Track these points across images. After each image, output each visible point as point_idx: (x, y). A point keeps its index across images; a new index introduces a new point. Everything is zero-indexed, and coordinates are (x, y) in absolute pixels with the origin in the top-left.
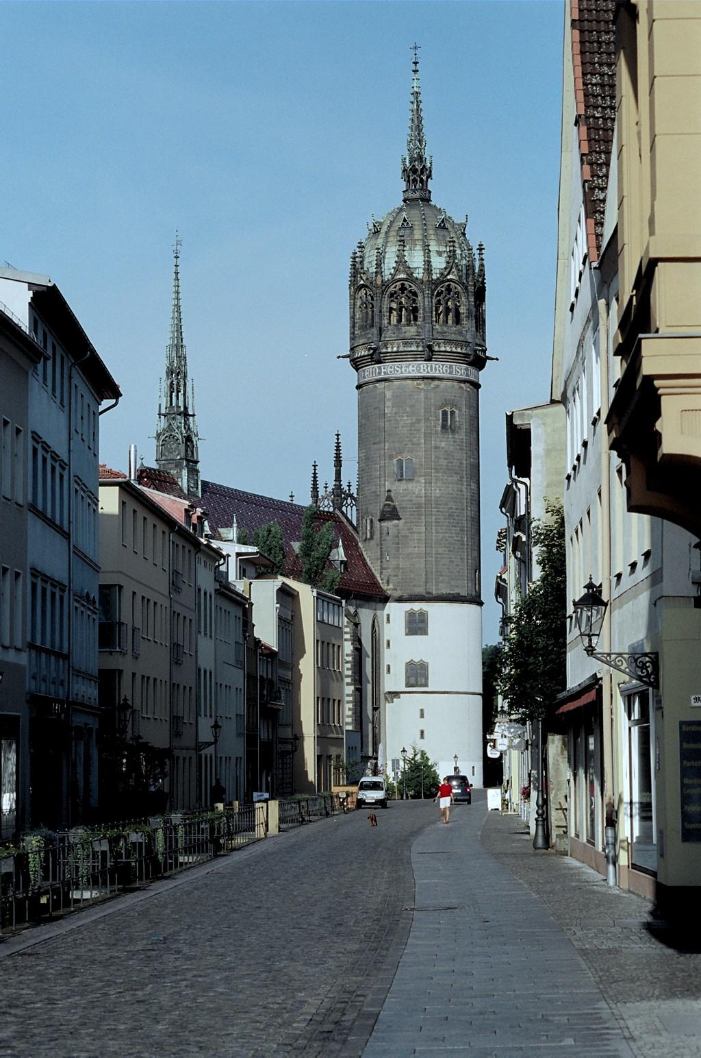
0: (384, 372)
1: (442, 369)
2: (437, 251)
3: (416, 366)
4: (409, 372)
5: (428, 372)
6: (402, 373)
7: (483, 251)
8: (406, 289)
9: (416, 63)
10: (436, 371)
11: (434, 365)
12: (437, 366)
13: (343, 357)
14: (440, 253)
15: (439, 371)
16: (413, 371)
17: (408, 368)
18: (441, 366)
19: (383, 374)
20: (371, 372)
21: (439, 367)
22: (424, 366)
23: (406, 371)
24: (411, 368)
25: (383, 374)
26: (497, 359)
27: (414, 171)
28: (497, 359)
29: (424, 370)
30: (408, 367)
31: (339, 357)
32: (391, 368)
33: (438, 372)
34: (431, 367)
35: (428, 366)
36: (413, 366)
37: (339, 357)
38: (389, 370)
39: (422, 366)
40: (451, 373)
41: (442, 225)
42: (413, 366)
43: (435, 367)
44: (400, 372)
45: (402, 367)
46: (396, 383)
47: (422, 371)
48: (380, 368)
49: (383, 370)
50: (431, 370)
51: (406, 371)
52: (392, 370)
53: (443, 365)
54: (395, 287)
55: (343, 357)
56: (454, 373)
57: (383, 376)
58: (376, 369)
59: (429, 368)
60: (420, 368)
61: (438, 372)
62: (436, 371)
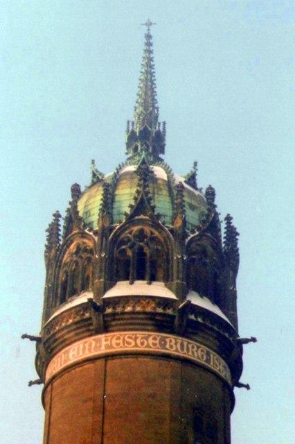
0: (107, 347)
1: (197, 351)
2: (188, 203)
3: (158, 339)
5: (177, 350)
6: (136, 345)
8: (146, 237)
9: (148, 37)
10: (188, 350)
11: (185, 344)
12: (190, 346)
13: (32, 338)
14: (192, 207)
15: (193, 353)
17: (147, 340)
18: (195, 349)
19: (103, 347)
20: (76, 352)
21: (193, 347)
22: (171, 341)
23: (142, 344)
24: (151, 341)
25: (103, 347)
27: (145, 134)
29: (171, 347)
30: (147, 339)
31: (25, 336)
32: (118, 338)
33: (190, 353)
34: (182, 345)
35: (176, 344)
36: (155, 339)
37: (25, 336)
38: (114, 341)
39: (168, 340)
40: (208, 361)
41: (192, 182)
43: (187, 346)
44: (133, 344)
45: (136, 339)
46: (125, 360)
47: (168, 346)
48: (99, 341)
49: (104, 343)
50: (182, 349)
52: (121, 341)
53: (198, 347)
54: (130, 233)
55: (32, 338)
56: (212, 364)
57: (103, 351)
58: (90, 345)
59: (179, 346)
60: (166, 343)
61: (190, 353)
62: (188, 350)
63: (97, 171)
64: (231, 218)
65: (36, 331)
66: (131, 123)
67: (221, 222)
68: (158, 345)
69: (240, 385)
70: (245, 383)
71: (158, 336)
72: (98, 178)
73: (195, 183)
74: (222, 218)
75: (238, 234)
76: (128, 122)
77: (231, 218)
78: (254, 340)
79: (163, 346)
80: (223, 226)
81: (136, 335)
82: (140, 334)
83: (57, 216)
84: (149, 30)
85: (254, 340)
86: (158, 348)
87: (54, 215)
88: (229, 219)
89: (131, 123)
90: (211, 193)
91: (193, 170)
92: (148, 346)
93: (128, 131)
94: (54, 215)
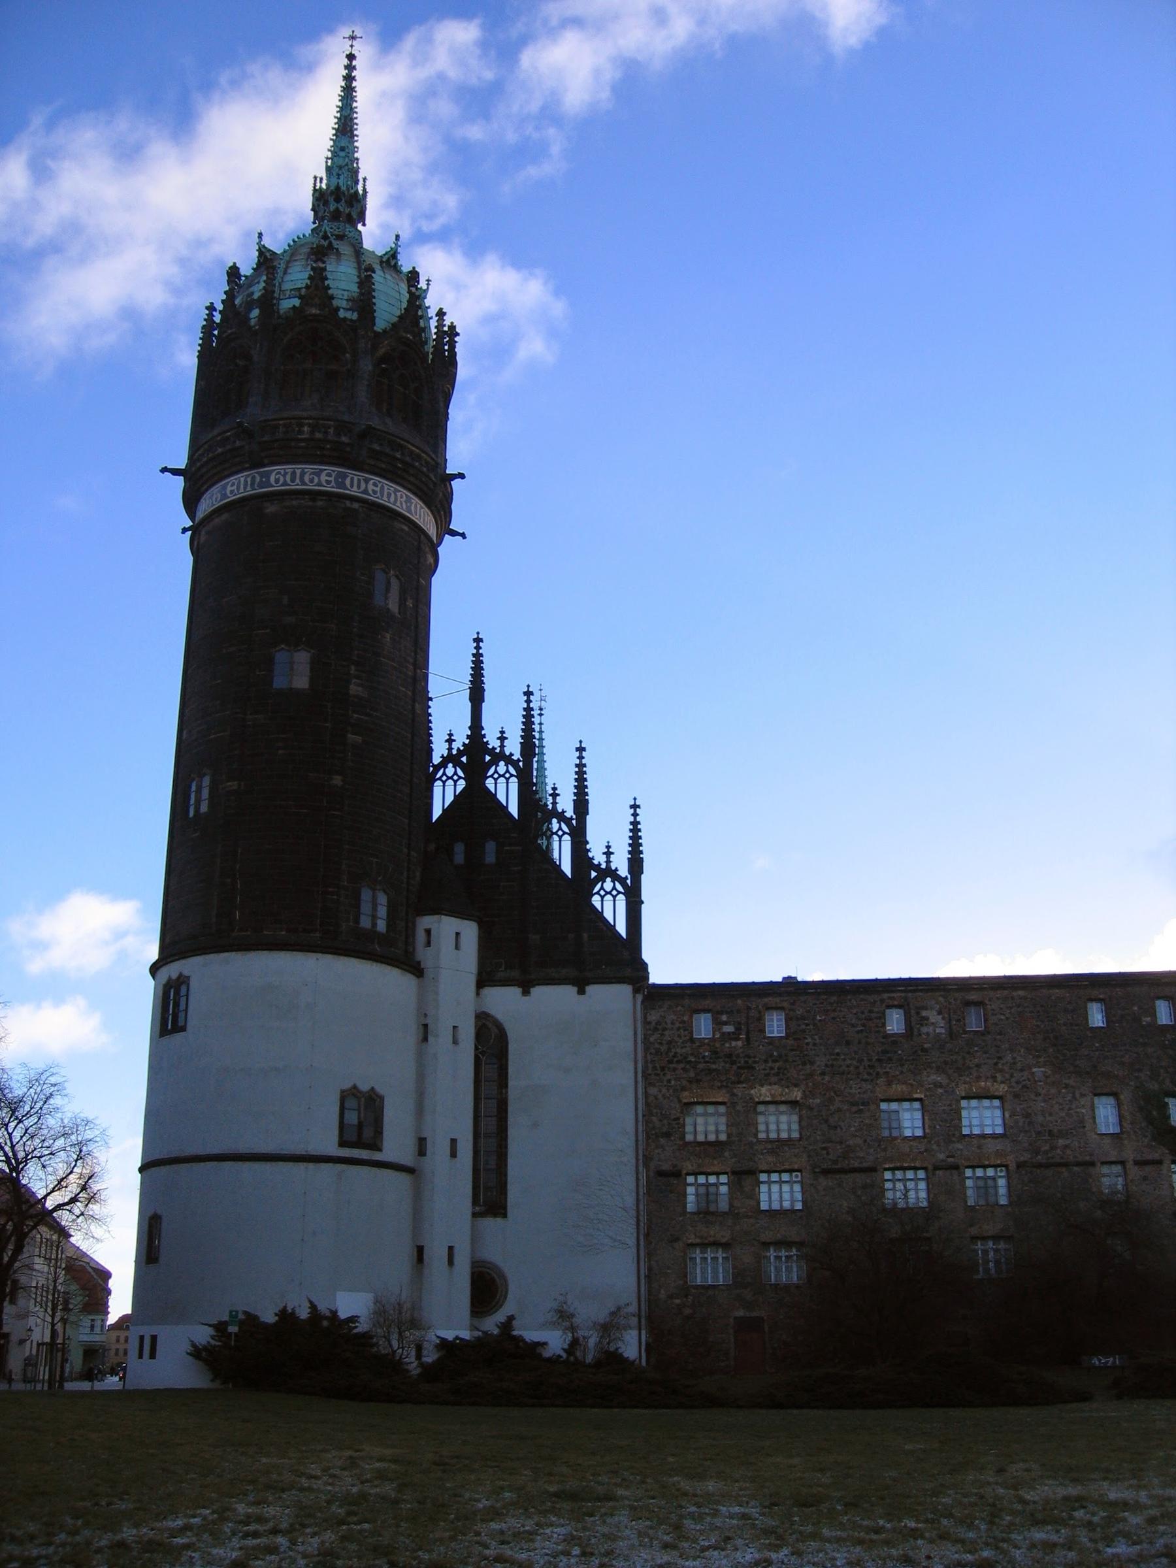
3: (334, 474)
4: (319, 484)
7: (456, 339)
13: (176, 472)
16: (328, 482)
23: (312, 481)
24: (324, 478)
26: (463, 536)
28: (463, 536)
30: (318, 474)
31: (165, 470)
37: (165, 470)
41: (393, 263)
42: (329, 475)
51: (312, 481)
55: (176, 472)
63: (264, 246)
64: (445, 314)
65: (182, 464)
66: (318, 180)
67: (431, 318)
68: (333, 484)
69: (454, 533)
70: (461, 532)
71: (334, 471)
72: (266, 257)
73: (396, 263)
74: (432, 312)
75: (458, 334)
76: (315, 178)
77: (445, 314)
78: (461, 476)
79: (342, 485)
80: (433, 323)
81: (303, 469)
82: (309, 468)
83: (211, 308)
84: (352, 46)
85: (461, 476)
86: (333, 487)
87: (207, 308)
88: (441, 314)
89: (318, 180)
90: (413, 276)
91: (393, 246)
92: (319, 484)
93: (315, 190)
94: (207, 308)
